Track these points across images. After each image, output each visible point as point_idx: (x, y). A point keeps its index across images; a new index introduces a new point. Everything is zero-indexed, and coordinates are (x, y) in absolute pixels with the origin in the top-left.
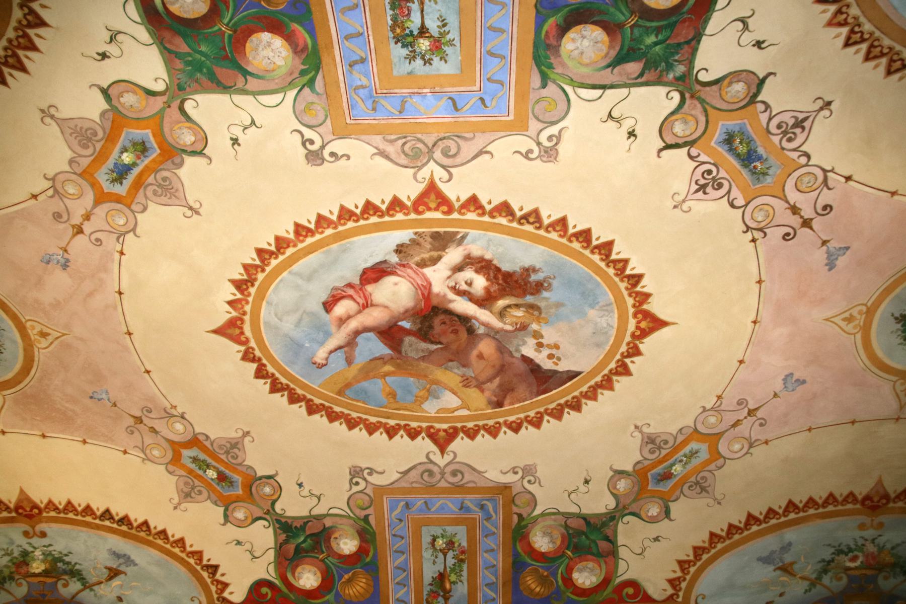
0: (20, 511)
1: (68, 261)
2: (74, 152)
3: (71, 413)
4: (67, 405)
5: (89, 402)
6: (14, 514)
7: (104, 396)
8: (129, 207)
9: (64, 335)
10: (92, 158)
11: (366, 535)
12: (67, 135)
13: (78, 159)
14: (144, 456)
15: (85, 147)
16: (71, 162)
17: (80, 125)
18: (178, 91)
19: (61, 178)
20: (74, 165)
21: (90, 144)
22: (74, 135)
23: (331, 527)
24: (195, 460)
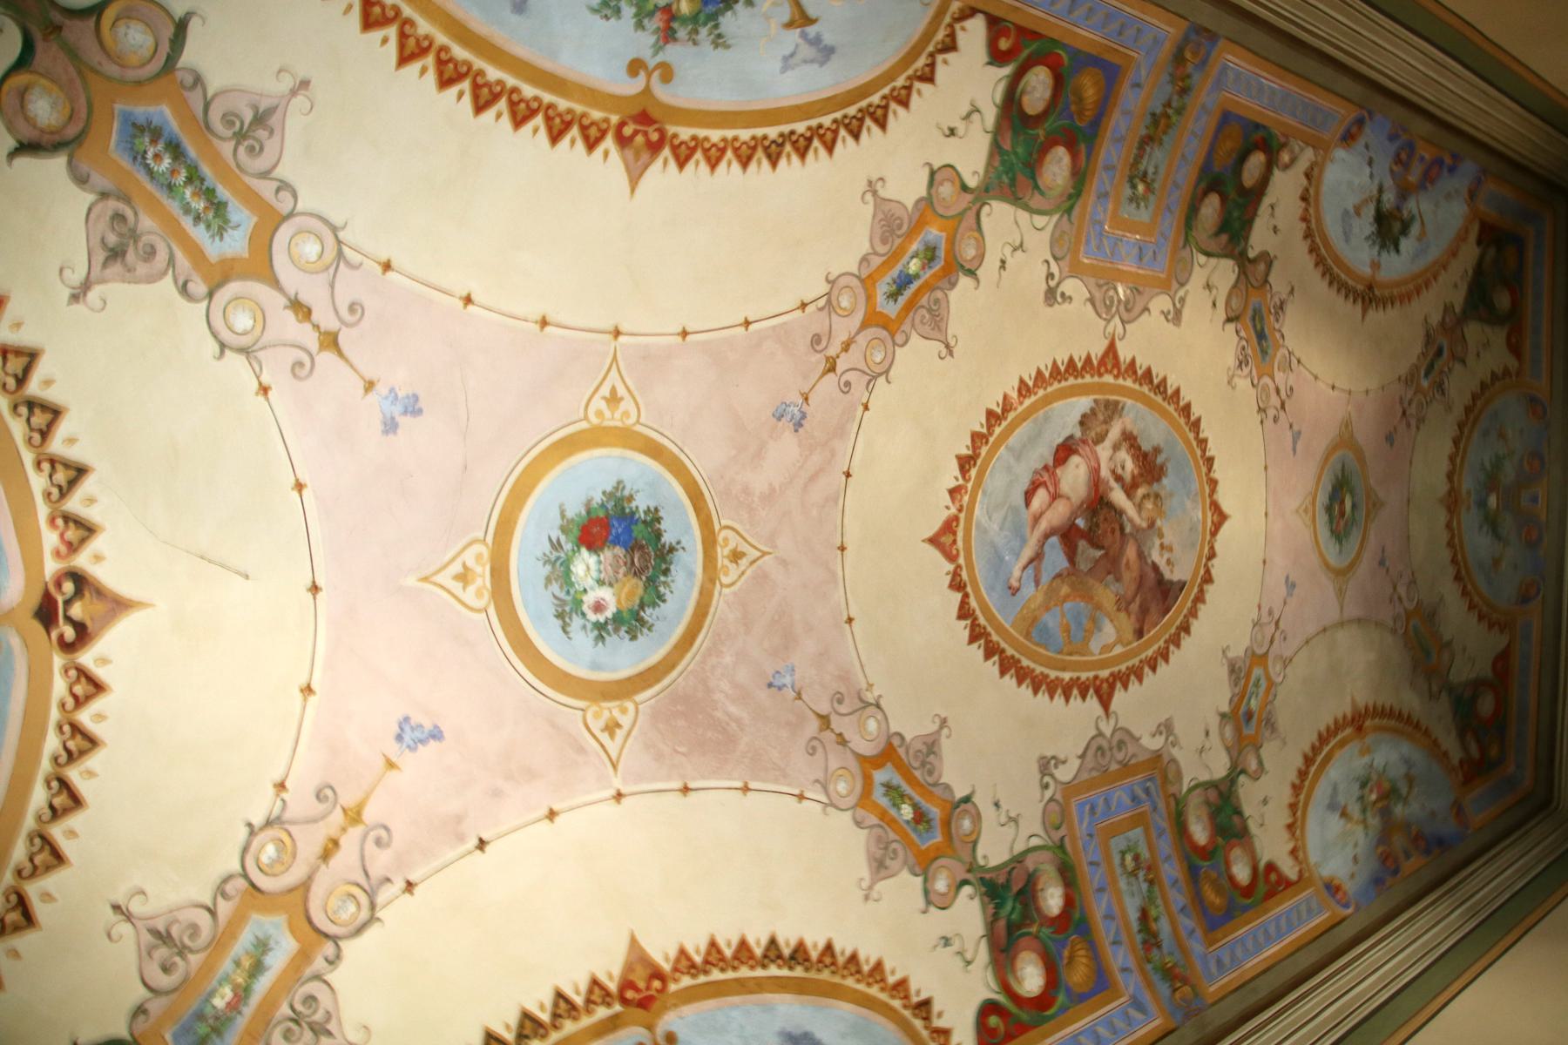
0: (630, 994)
1: (804, 416)
3: (734, 725)
4: (733, 709)
5: (763, 695)
6: (618, 1008)
7: (787, 680)
8: (893, 336)
9: (764, 554)
11: (1067, 874)
14: (824, 799)
18: (986, 192)
19: (843, 281)
23: (1035, 871)
24: (889, 787)
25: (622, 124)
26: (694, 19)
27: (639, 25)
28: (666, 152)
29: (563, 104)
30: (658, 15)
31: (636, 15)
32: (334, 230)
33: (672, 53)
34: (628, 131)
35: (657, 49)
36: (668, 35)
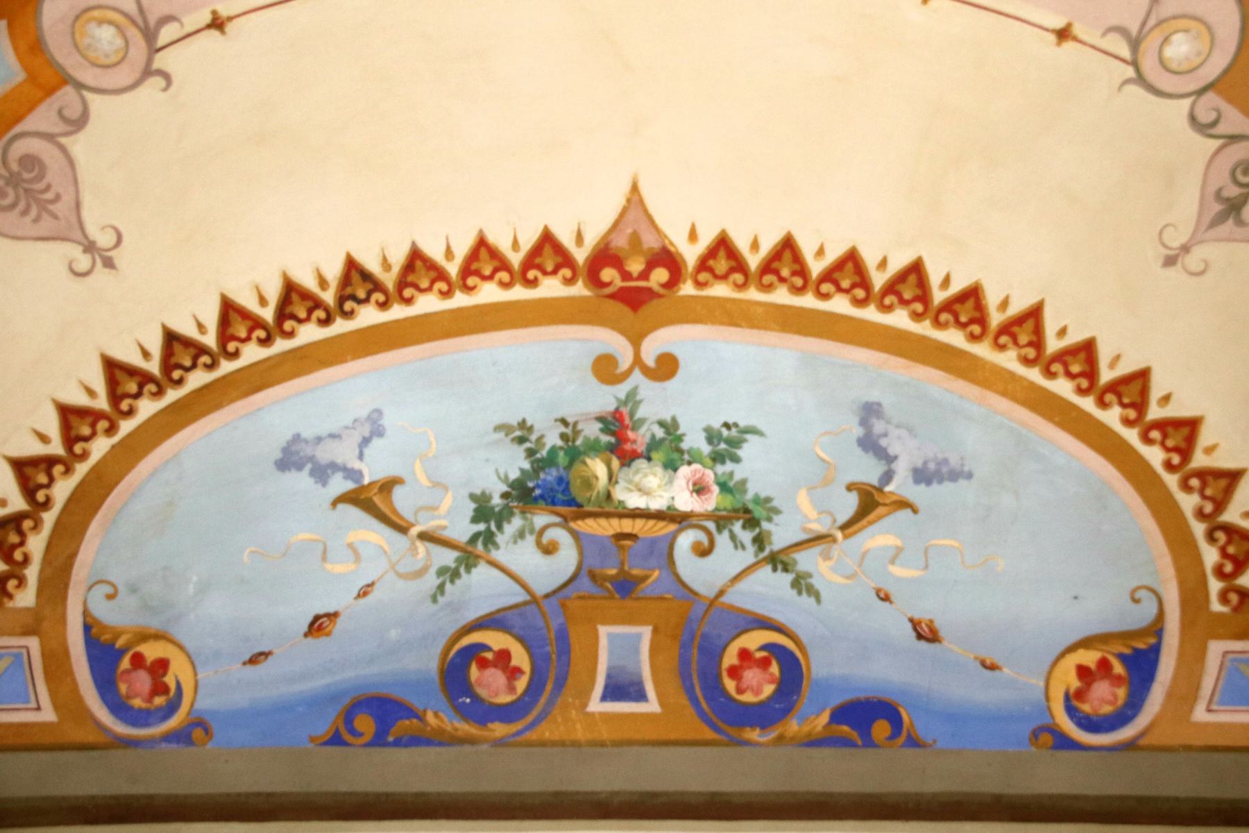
2: (63, 149)
10: (18, 129)
12: (68, 198)
13: (60, 127)
15: (30, 161)
16: (79, 123)
17: (28, 219)
19: (123, 76)
20: (74, 112)
21: (15, 167)
22: (49, 196)
25: (673, 283)
26: (575, 455)
27: (670, 427)
28: (581, 256)
29: (781, 296)
30: (641, 448)
31: (680, 438)
32: (1140, 79)
33: (605, 399)
34: (660, 275)
35: (632, 397)
36: (617, 425)
